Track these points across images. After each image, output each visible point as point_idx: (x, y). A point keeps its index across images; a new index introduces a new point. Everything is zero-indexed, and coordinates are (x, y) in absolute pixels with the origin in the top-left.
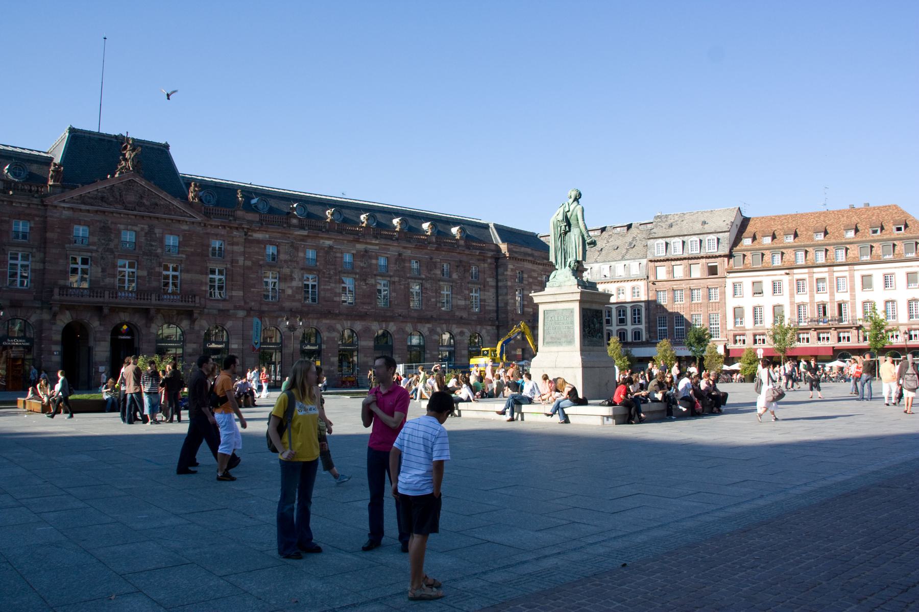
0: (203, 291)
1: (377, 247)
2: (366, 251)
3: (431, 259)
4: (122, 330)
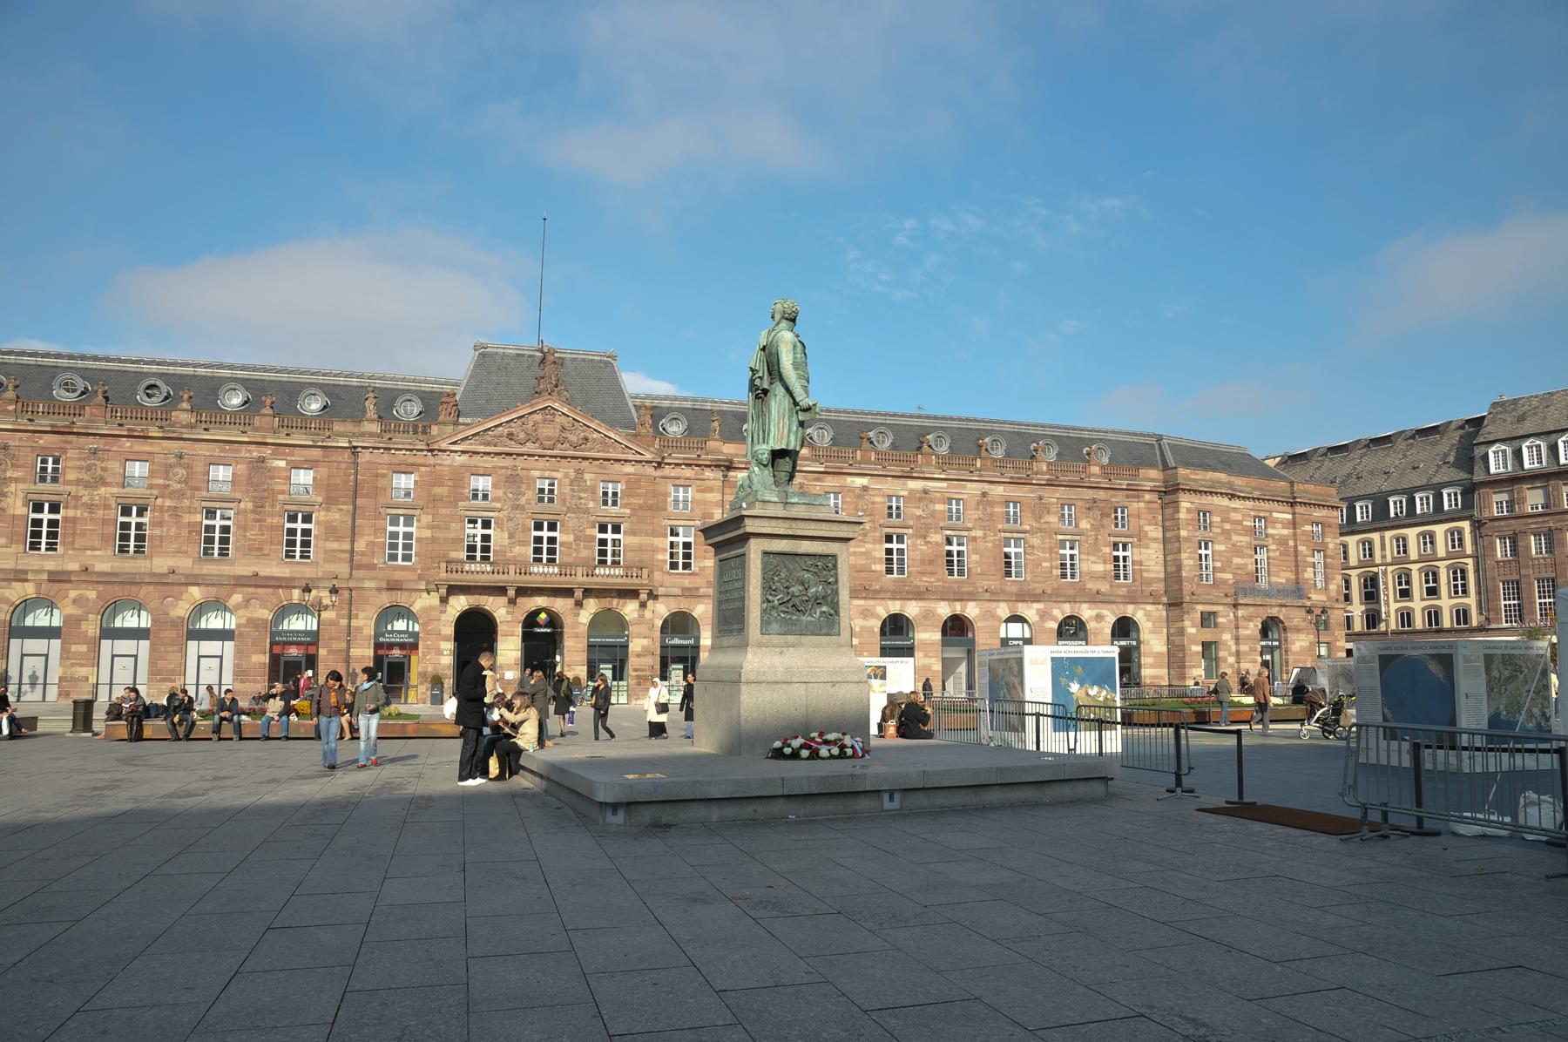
0: (661, 561)
1: (944, 484)
2: (925, 492)
3: (1040, 498)
4: (538, 619)
